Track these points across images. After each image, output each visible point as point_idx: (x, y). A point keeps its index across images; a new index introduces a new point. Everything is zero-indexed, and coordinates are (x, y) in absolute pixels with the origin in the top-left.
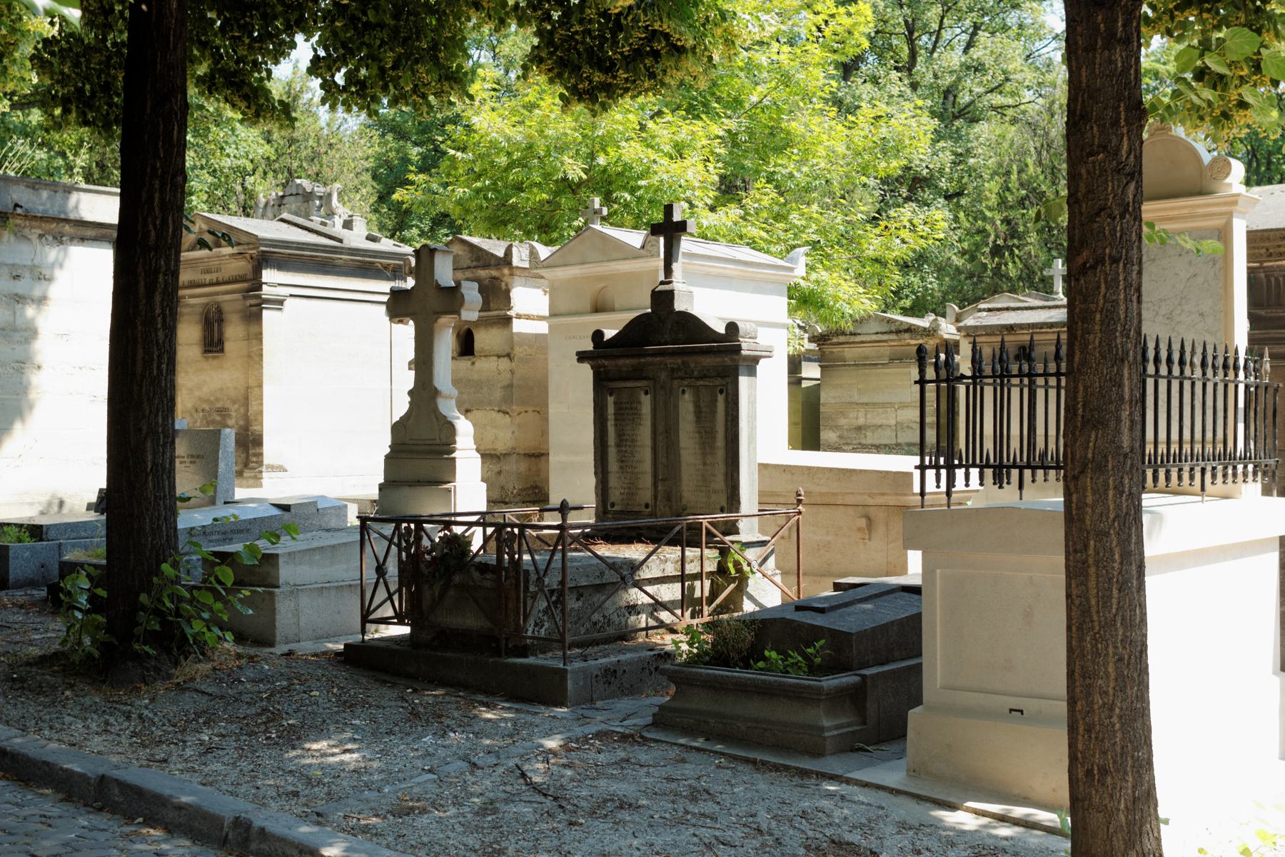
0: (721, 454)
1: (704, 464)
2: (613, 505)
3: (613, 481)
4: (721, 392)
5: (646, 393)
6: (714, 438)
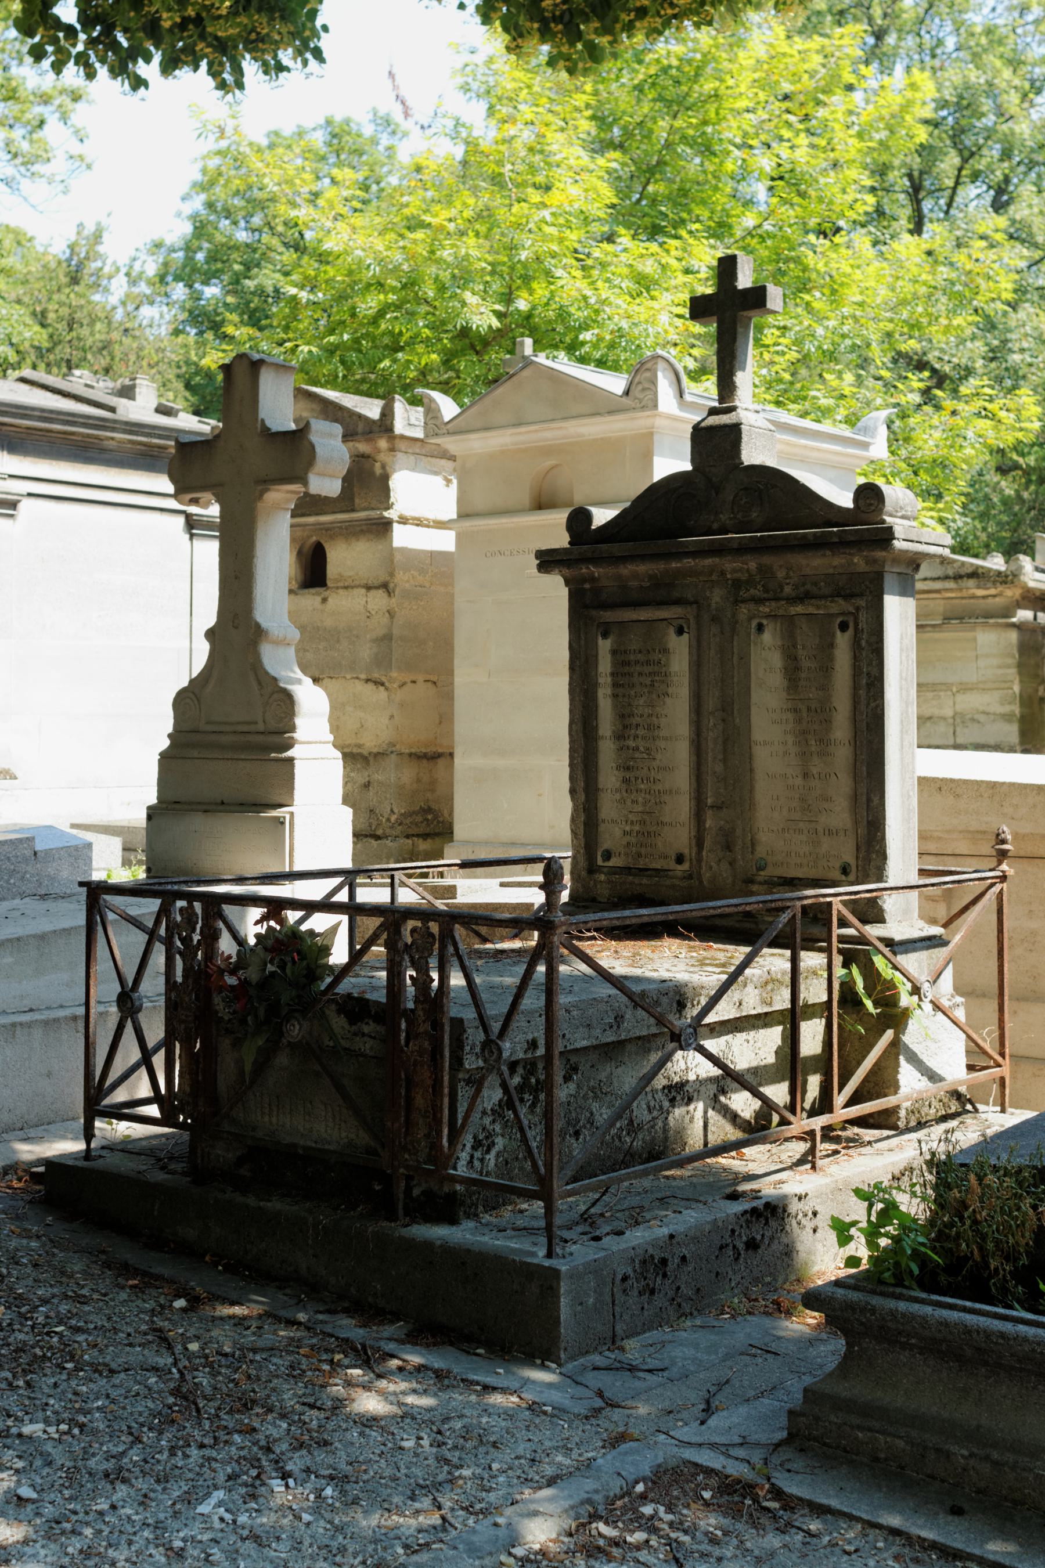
0: (842, 754)
1: (806, 775)
2: (608, 855)
3: (608, 808)
4: (844, 627)
5: (680, 631)
6: (828, 721)
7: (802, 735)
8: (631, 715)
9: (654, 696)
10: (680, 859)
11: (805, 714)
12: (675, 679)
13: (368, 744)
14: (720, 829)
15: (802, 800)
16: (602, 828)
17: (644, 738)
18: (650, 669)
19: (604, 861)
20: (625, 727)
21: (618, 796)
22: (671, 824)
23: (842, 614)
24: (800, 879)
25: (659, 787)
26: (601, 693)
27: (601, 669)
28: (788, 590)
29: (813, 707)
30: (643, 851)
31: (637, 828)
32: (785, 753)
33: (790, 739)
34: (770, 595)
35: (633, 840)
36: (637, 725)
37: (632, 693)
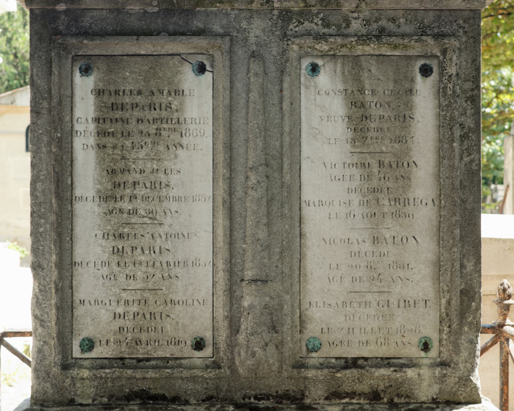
0: (424, 215)
1: (375, 240)
2: (89, 345)
3: (89, 284)
4: (426, 71)
5: (201, 69)
6: (406, 178)
7: (373, 194)
8: (126, 170)
9: (161, 148)
10: (199, 345)
11: (375, 170)
12: (192, 127)
13: (77, 205)
14: (266, 307)
15: (370, 268)
16: (79, 311)
17: (145, 198)
18: (155, 114)
19: (83, 351)
20: (116, 185)
21: (105, 271)
22: (185, 303)
23: (425, 56)
24: (366, 359)
25: (169, 258)
26: (78, 143)
27: (78, 113)
28: (356, 25)
29: (387, 161)
30: (144, 336)
31: (135, 308)
32: (348, 215)
33: (356, 198)
34: (333, 30)
35: (129, 324)
36: (135, 184)
37: (128, 143)
